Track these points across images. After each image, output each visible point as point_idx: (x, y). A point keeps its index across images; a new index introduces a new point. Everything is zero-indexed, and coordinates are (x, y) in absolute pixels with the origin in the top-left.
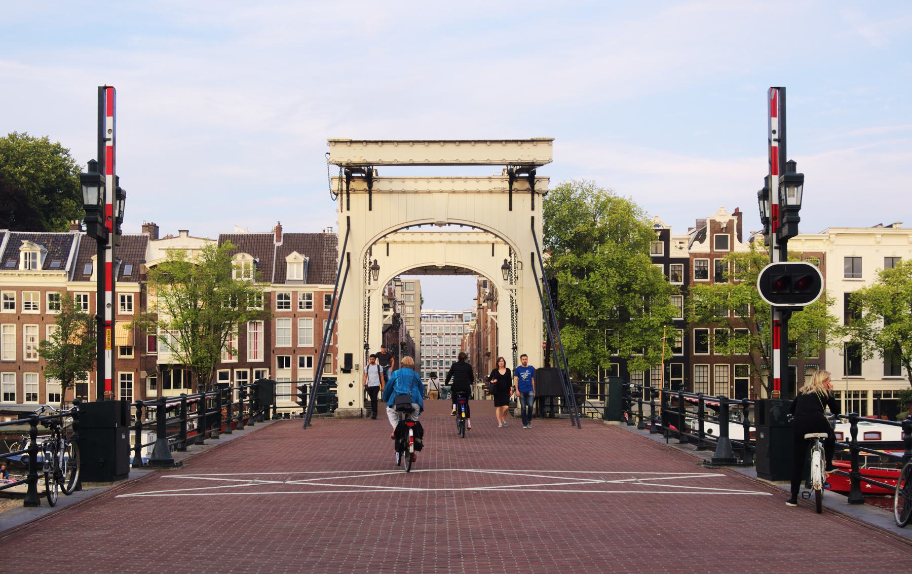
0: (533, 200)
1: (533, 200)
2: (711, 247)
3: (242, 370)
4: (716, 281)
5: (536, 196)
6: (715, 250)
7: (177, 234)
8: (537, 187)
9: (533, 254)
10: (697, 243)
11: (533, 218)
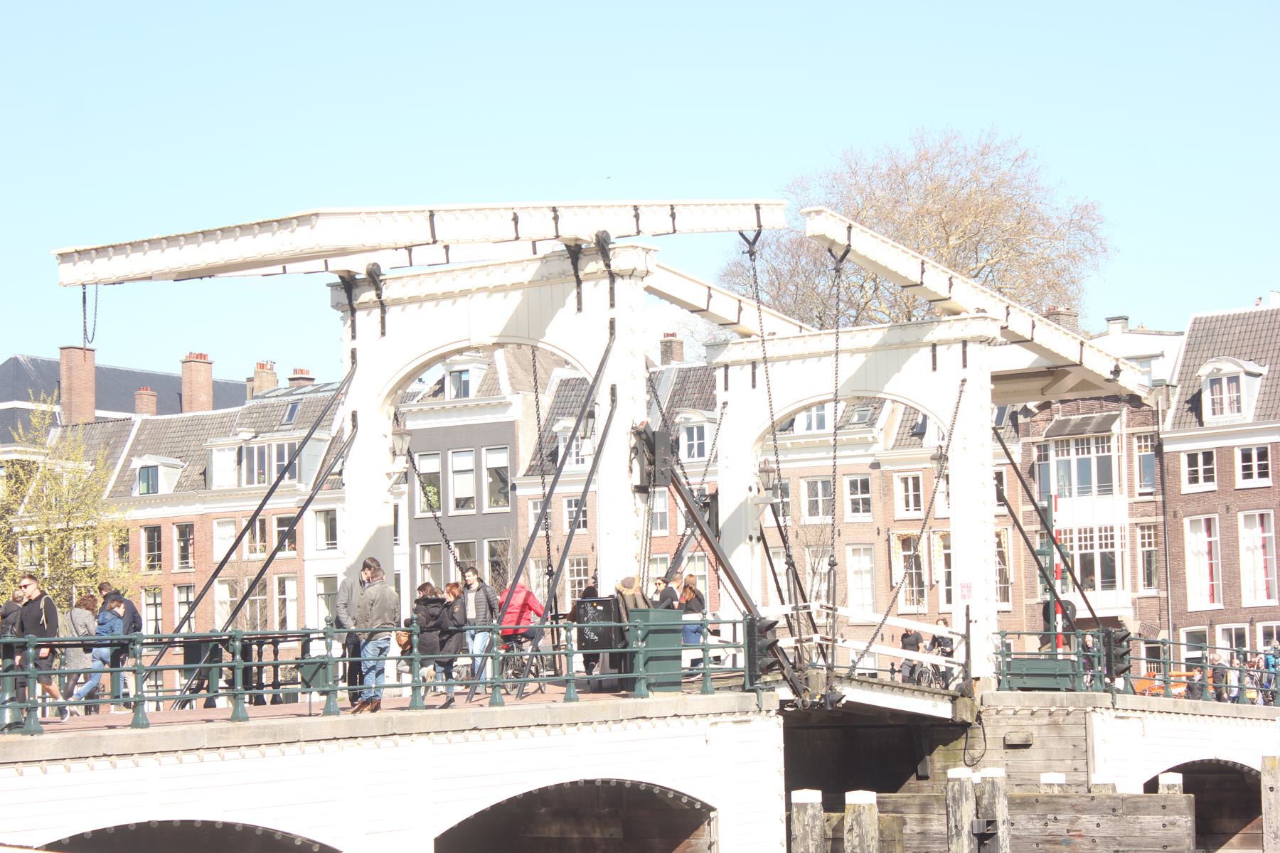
0: (612, 289)
1: (612, 289)
3: (1233, 626)
5: (619, 281)
7: (1103, 326)
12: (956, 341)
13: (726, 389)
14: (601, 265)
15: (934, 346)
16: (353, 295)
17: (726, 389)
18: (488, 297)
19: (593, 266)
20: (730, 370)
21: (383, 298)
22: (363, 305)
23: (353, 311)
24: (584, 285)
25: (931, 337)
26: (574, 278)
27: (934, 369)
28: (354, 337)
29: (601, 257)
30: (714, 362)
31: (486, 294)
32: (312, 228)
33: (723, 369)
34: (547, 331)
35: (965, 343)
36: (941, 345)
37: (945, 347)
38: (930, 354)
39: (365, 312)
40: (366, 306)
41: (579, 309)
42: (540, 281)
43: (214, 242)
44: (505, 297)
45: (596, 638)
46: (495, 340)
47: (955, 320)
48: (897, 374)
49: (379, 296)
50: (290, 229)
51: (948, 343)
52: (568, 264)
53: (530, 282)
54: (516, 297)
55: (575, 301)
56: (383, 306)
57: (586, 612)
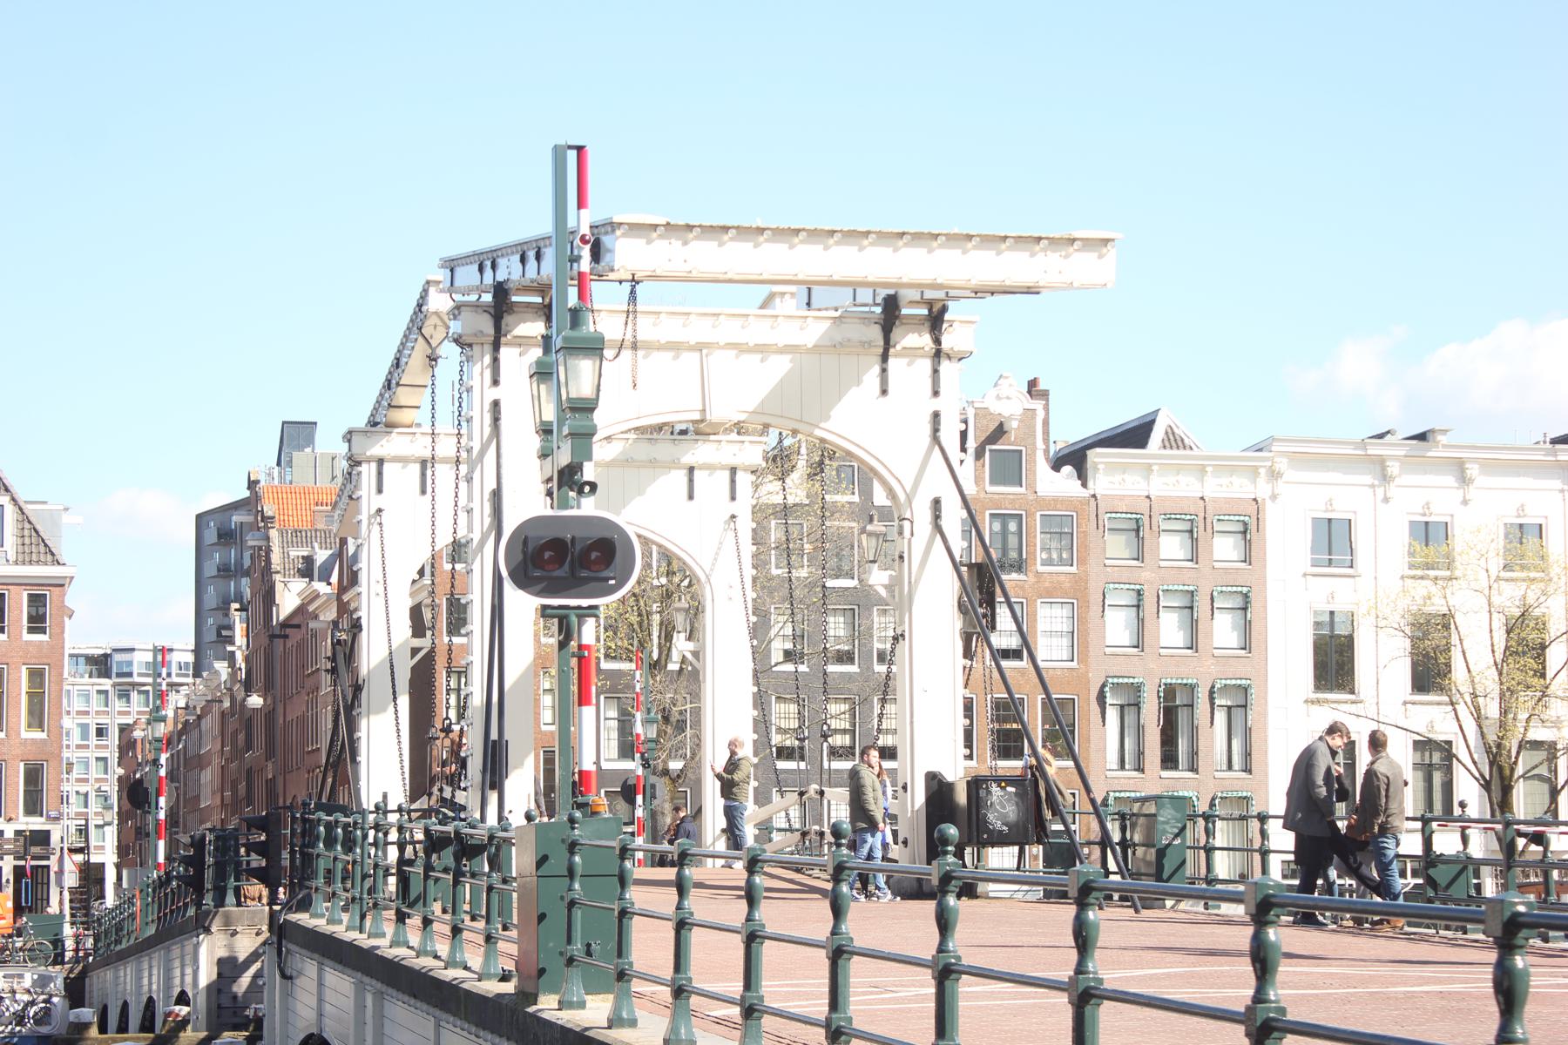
0: (936, 371)
1: (936, 371)
5: (945, 366)
8: (947, 342)
9: (937, 503)
11: (936, 415)
12: (723, 468)
13: (380, 491)
14: (924, 340)
15: (691, 470)
16: (503, 326)
17: (380, 491)
18: (737, 357)
19: (915, 340)
20: (386, 466)
22: (518, 340)
24: (891, 361)
25: (688, 459)
26: (882, 350)
27: (691, 497)
28: (496, 382)
30: (368, 454)
31: (735, 352)
32: (1100, 257)
33: (374, 465)
34: (832, 413)
35: (733, 471)
36: (700, 469)
38: (685, 480)
39: (517, 350)
41: (884, 392)
42: (829, 348)
43: (856, 248)
44: (762, 361)
45: (1005, 828)
47: (751, 442)
48: (639, 498)
50: (1063, 253)
52: (876, 333)
53: (815, 346)
54: (780, 366)
55: (877, 382)
57: (989, 792)
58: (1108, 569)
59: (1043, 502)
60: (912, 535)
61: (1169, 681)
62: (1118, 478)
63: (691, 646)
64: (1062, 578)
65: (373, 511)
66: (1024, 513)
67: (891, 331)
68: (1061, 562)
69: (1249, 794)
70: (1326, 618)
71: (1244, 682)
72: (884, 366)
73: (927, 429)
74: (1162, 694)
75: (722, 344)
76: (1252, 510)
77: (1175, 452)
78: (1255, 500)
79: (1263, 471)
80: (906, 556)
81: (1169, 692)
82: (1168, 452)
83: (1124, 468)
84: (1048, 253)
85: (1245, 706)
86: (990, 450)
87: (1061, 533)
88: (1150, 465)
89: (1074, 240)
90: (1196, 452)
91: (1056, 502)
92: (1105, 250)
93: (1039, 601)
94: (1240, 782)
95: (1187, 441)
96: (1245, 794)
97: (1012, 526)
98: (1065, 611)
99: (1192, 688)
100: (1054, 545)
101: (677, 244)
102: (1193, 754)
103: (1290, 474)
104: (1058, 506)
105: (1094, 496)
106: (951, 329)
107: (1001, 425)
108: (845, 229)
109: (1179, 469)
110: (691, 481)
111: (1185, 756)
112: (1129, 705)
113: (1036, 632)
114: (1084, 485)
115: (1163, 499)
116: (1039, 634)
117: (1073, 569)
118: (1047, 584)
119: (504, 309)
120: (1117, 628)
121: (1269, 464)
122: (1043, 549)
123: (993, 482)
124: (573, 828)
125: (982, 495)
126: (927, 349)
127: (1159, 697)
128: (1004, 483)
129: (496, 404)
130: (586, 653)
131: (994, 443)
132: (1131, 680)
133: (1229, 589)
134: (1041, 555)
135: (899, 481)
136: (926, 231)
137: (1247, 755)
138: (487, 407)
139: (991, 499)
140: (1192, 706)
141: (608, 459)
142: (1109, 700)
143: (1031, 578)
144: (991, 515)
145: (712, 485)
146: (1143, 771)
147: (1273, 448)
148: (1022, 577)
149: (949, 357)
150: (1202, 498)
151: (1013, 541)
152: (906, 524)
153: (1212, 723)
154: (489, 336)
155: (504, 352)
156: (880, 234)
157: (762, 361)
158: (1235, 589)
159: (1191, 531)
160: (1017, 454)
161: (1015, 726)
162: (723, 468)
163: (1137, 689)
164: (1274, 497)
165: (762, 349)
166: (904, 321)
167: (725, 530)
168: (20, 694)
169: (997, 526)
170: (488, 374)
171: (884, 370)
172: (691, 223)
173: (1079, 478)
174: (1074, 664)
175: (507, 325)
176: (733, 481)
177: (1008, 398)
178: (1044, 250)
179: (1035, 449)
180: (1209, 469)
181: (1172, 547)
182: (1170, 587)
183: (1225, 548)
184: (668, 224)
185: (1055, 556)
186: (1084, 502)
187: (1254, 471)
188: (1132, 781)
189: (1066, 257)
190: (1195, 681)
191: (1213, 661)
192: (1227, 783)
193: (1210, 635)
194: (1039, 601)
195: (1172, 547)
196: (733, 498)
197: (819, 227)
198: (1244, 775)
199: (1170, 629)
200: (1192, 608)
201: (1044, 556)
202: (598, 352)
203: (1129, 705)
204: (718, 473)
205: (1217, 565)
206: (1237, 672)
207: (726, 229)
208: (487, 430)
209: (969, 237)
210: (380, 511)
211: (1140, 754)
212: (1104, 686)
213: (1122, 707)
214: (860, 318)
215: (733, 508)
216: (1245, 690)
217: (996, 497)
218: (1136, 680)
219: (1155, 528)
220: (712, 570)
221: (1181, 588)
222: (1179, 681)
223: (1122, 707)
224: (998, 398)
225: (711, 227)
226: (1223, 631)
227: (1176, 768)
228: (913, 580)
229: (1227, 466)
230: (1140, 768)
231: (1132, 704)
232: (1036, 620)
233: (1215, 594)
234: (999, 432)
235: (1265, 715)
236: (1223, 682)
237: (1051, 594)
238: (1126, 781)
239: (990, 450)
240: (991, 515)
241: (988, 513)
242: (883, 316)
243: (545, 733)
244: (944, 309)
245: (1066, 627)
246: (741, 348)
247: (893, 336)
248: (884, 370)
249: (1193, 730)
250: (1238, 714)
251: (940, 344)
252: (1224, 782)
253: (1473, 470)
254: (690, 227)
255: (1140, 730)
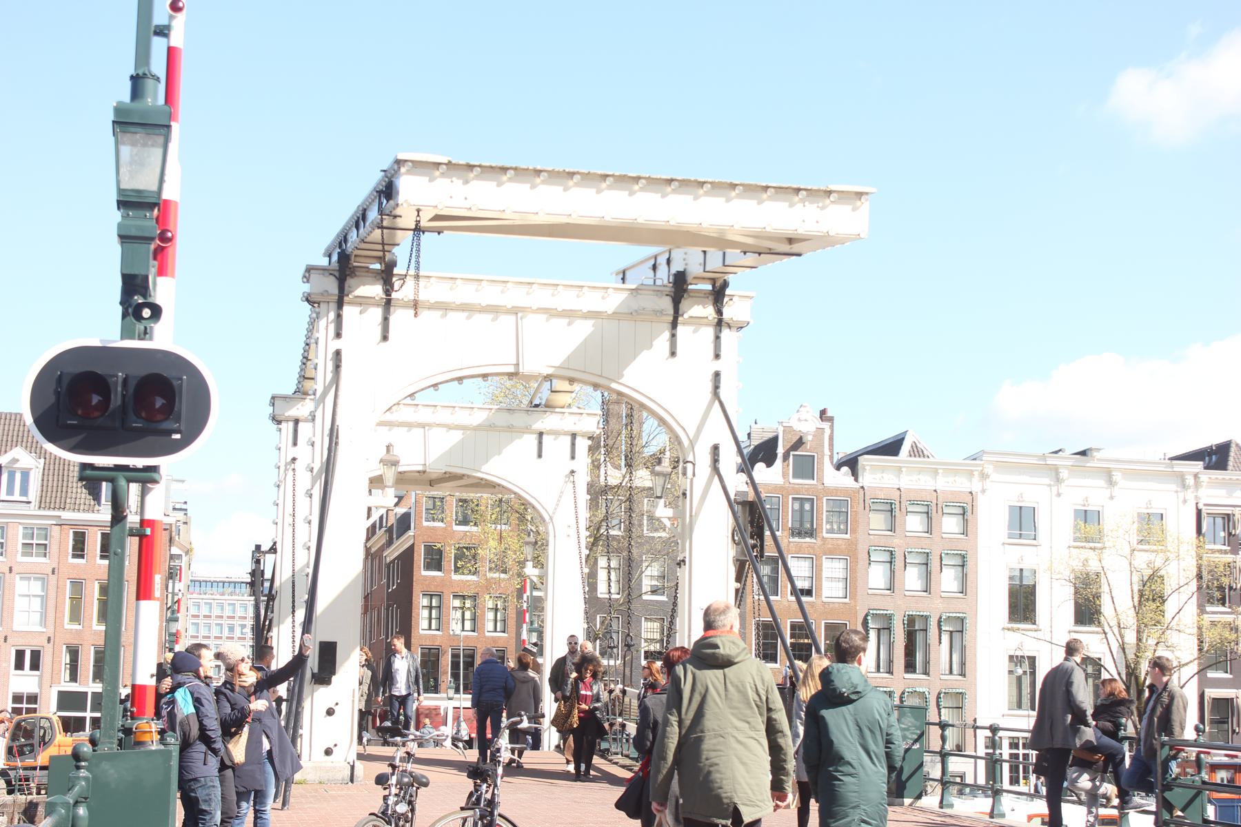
0: (717, 338)
1: (717, 338)
2: (785, 475)
4: (793, 535)
5: (726, 334)
6: (792, 480)
8: (727, 313)
9: (716, 448)
10: (760, 466)
11: (717, 375)
12: (565, 433)
14: (709, 311)
15: (541, 434)
16: (346, 288)
17: (295, 444)
18: (548, 320)
20: (300, 425)
21: (394, 295)
22: (358, 300)
23: (340, 304)
24: (680, 328)
25: (538, 426)
26: (672, 318)
27: (540, 456)
28: (338, 335)
29: (711, 303)
30: (286, 414)
32: (854, 209)
33: (291, 424)
34: (624, 373)
35: (574, 436)
36: (548, 434)
37: (552, 437)
38: (536, 442)
39: (357, 309)
40: (364, 302)
41: (673, 354)
46: (550, 371)
49: (388, 292)
50: (820, 205)
51: (556, 433)
52: (667, 304)
53: (613, 313)
54: (584, 328)
56: (388, 304)
58: (871, 537)
59: (828, 491)
60: (694, 475)
61: (911, 613)
62: (879, 476)
63: (536, 572)
64: (840, 542)
65: (289, 459)
66: (815, 498)
67: (680, 302)
68: (839, 531)
69: (964, 691)
70: (1018, 573)
71: (961, 615)
72: (674, 332)
73: (709, 387)
74: (906, 622)
75: (534, 308)
76: (968, 499)
77: (917, 459)
78: (971, 493)
79: (976, 473)
80: (688, 493)
81: (911, 620)
82: (913, 459)
83: (883, 469)
84: (807, 203)
85: (962, 632)
86: (793, 455)
87: (840, 512)
88: (901, 468)
89: (829, 193)
90: (931, 459)
91: (836, 490)
92: (859, 203)
93: (824, 557)
94: (958, 683)
95: (925, 452)
96: (961, 691)
97: (807, 507)
98: (842, 564)
99: (926, 618)
100: (835, 519)
101: (458, 182)
102: (926, 663)
103: (994, 476)
104: (839, 494)
105: (862, 487)
106: (731, 302)
107: (801, 438)
108: (617, 174)
109: (921, 471)
110: (540, 443)
111: (921, 664)
112: (884, 629)
113: (821, 578)
114: (856, 480)
115: (909, 490)
116: (824, 579)
117: (848, 536)
118: (830, 546)
119: (348, 273)
120: (877, 576)
121: (981, 468)
122: (827, 522)
123: (795, 476)
124: (78, 768)
125: (787, 485)
126: (710, 318)
127: (904, 624)
128: (802, 477)
129: (338, 353)
130: (148, 531)
131: (796, 450)
132: (885, 612)
133: (953, 552)
134: (826, 527)
135: (684, 430)
136: (692, 179)
137: (963, 664)
138: (330, 356)
139: (793, 488)
140: (926, 630)
141: (475, 425)
142: (870, 625)
143: (819, 542)
144: (793, 499)
145: (557, 447)
146: (892, 673)
147: (984, 458)
148: (813, 540)
149: (729, 326)
150: (935, 491)
151: (807, 517)
152: (689, 466)
153: (940, 643)
154: (332, 295)
155: (347, 310)
156: (649, 179)
157: (569, 324)
158: (956, 552)
159: (928, 513)
160: (811, 458)
161: (806, 641)
162: (565, 433)
163: (889, 618)
164: (983, 491)
165: (570, 315)
166: (691, 294)
167: (566, 482)
168: (65, 598)
169: (797, 506)
170: (332, 328)
171: (673, 336)
172: (472, 163)
173: (853, 475)
174: (847, 600)
175: (349, 287)
176: (573, 444)
177: (806, 420)
178: (803, 201)
179: (823, 455)
180: (940, 471)
181: (914, 523)
182: (913, 550)
183: (950, 525)
184: (450, 162)
185: (835, 527)
186: (856, 491)
187: (971, 473)
188: (885, 680)
189: (823, 208)
190: (928, 614)
191: (941, 600)
192: (949, 682)
193: (939, 583)
194: (824, 557)
195: (914, 523)
196: (573, 458)
197: (592, 171)
198: (960, 678)
199: (912, 579)
200: (927, 564)
201: (828, 527)
202: (163, 131)
203: (884, 629)
204: (562, 437)
205: (944, 536)
206: (955, 608)
207: (504, 170)
208: (329, 376)
209: (733, 186)
210: (294, 459)
211: (890, 662)
212: (867, 615)
213: (879, 630)
214: (654, 291)
215: (573, 465)
216: (962, 620)
217: (797, 486)
218: (889, 612)
219: (903, 510)
220: (554, 513)
221: (920, 550)
222: (918, 613)
223: (879, 630)
224: (799, 420)
225: (491, 167)
226: (948, 580)
227: (914, 672)
228: (694, 514)
229: (953, 469)
230: (890, 672)
231: (886, 628)
232: (822, 570)
233: (943, 555)
234: (799, 443)
235: (975, 638)
236: (948, 614)
237: (832, 552)
238: (881, 680)
239: (793, 455)
240: (793, 499)
241: (791, 497)
242: (673, 290)
243: (488, 638)
244: (725, 285)
245: (841, 575)
246: (551, 313)
247: (681, 306)
248: (673, 336)
249: (927, 646)
250: (957, 636)
251: (721, 314)
252: (949, 682)
253: (1117, 476)
254: (470, 167)
255: (890, 646)
